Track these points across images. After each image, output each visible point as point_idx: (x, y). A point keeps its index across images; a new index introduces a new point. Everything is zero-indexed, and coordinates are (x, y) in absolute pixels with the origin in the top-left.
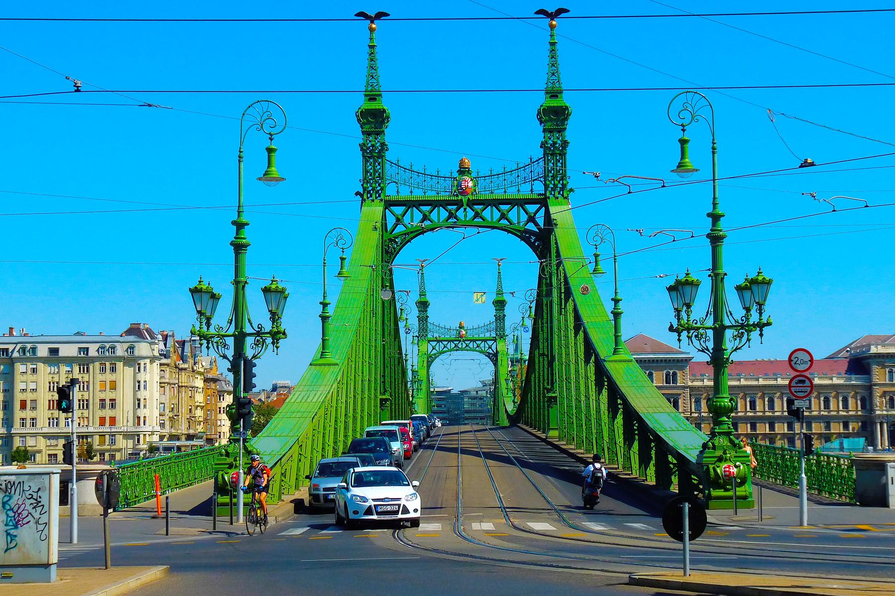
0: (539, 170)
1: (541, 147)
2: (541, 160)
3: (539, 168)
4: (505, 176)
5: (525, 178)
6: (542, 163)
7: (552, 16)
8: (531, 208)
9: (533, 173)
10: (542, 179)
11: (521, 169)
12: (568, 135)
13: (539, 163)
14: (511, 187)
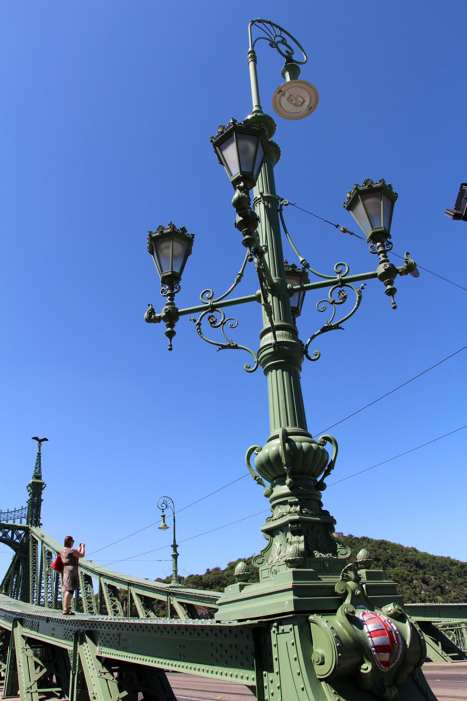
0: (26, 513)
1: (27, 502)
2: (27, 508)
3: (25, 512)
4: (8, 514)
5: (18, 516)
6: (27, 510)
7: (40, 441)
8: (21, 532)
9: (22, 514)
10: (26, 518)
11: (17, 512)
12: (43, 497)
13: (26, 509)
14: (10, 520)
